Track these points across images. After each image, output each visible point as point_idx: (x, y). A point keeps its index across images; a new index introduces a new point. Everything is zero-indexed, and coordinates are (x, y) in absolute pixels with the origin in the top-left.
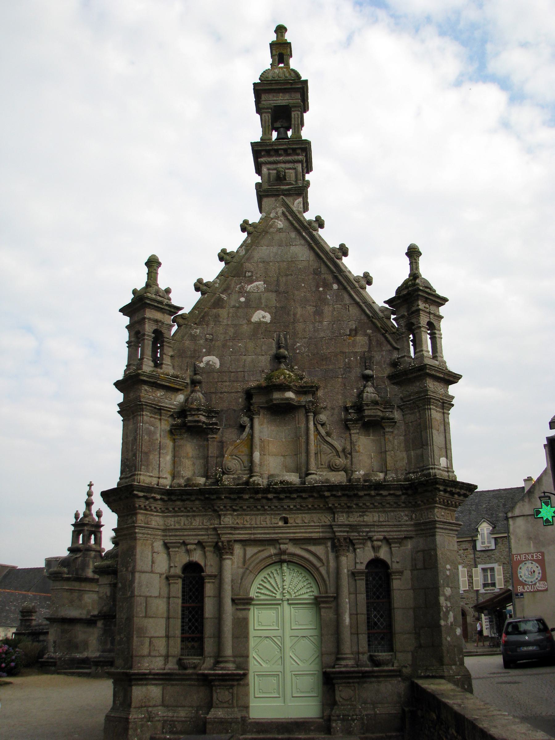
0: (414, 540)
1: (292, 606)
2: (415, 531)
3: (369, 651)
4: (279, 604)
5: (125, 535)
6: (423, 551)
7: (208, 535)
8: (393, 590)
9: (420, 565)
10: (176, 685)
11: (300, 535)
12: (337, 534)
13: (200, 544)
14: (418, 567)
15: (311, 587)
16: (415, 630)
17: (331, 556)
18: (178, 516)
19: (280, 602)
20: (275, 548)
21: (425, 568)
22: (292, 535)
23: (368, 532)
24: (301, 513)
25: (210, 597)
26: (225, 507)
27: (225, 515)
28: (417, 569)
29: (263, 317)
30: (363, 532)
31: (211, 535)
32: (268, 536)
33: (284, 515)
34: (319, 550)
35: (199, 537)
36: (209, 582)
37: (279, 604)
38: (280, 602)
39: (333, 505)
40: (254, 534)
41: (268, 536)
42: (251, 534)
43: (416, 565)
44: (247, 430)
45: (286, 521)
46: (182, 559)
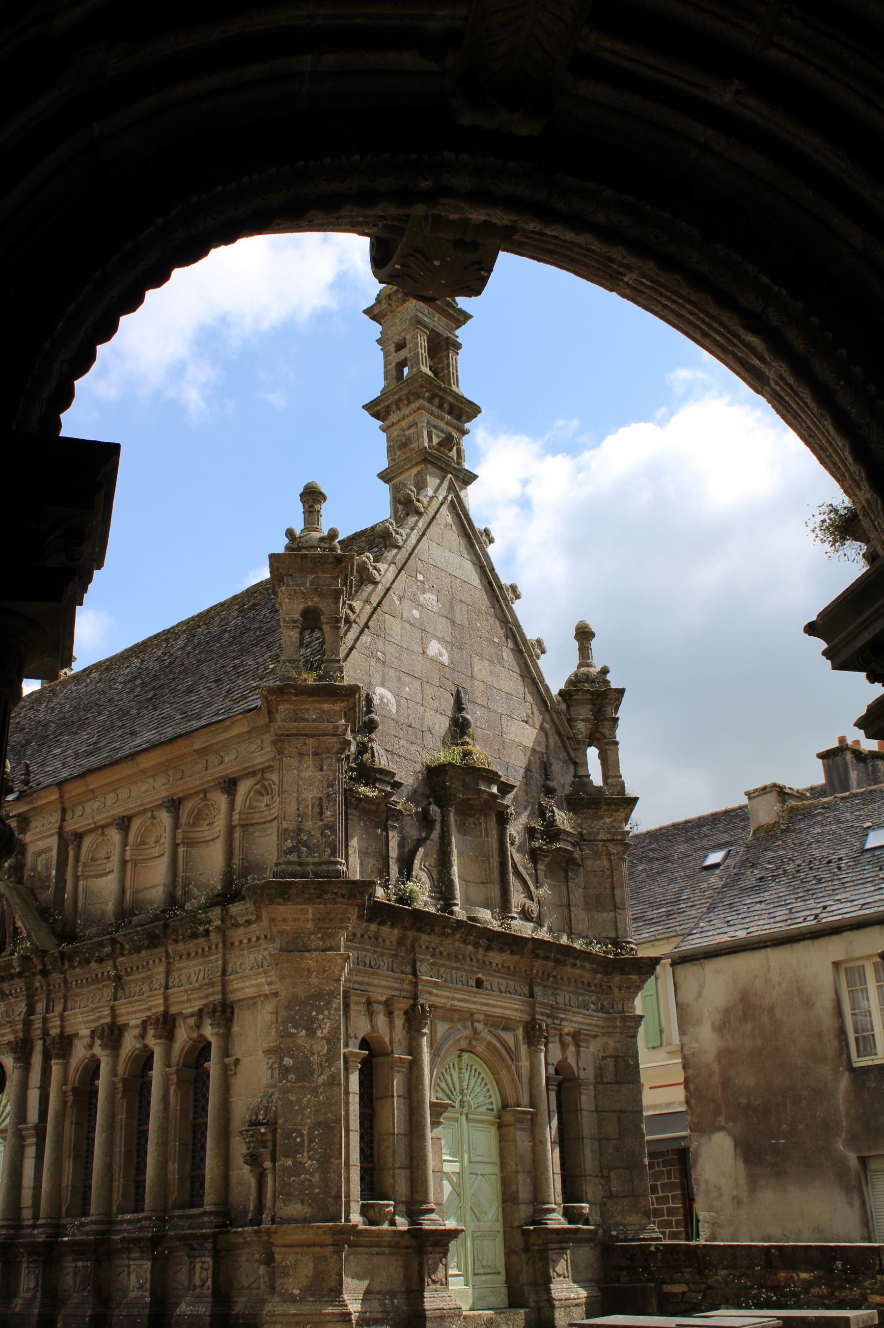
0: (598, 1039)
2: (603, 1027)
3: (564, 1202)
6: (616, 1057)
7: (401, 991)
8: (581, 1110)
9: (609, 1077)
10: (361, 1253)
11: (498, 1010)
12: (538, 1017)
14: (605, 1080)
16: (601, 1171)
17: (523, 1048)
18: (364, 949)
19: (458, 1115)
20: (465, 1027)
21: (618, 1082)
22: (490, 1009)
23: (562, 1020)
24: (497, 977)
28: (604, 1083)
29: (441, 655)
30: (558, 1018)
31: (406, 991)
32: (466, 1005)
33: (480, 975)
34: (508, 1037)
36: (398, 1072)
38: (458, 1115)
39: (537, 972)
40: (453, 999)
41: (466, 1005)
42: (448, 998)
43: (601, 1075)
44: (438, 826)
45: (479, 984)
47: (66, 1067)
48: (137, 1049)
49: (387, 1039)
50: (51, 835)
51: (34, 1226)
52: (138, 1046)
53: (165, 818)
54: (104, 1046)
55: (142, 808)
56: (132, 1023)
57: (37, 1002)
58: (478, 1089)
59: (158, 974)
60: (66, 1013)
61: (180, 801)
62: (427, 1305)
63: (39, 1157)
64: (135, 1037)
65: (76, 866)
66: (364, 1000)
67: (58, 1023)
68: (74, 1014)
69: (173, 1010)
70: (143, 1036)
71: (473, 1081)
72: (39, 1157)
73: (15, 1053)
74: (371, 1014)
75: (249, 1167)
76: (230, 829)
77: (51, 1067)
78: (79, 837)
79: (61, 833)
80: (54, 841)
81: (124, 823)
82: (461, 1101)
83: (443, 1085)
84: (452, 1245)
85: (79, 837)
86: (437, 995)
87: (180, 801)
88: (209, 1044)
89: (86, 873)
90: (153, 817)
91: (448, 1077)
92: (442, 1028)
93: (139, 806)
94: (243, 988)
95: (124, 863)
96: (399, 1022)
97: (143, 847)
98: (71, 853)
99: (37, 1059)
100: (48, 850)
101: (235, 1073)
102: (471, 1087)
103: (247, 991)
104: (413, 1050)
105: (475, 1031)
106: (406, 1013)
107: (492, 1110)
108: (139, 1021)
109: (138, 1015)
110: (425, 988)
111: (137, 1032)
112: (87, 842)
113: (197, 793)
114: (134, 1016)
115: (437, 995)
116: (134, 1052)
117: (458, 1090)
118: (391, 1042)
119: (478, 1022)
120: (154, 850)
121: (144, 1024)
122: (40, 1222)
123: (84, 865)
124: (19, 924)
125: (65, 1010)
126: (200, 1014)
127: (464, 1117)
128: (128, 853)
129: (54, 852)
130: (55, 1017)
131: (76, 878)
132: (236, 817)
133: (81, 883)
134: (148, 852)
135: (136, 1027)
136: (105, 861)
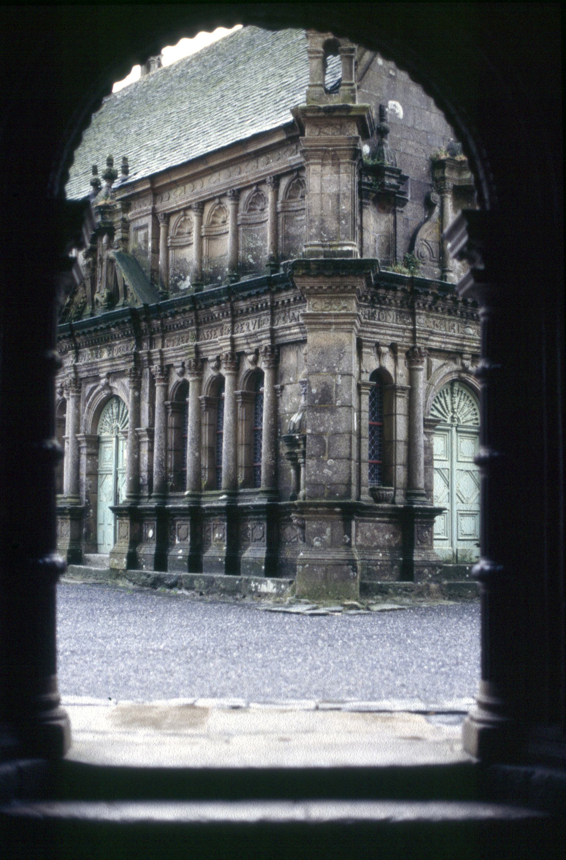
1: (459, 434)
4: (447, 431)
5: (330, 324)
13: (393, 348)
15: (476, 414)
19: (449, 428)
20: (456, 363)
25: (400, 414)
26: (424, 305)
27: (420, 314)
31: (406, 337)
35: (396, 339)
36: (400, 397)
37: (447, 431)
38: (449, 428)
44: (437, 209)
46: (371, 363)
47: (166, 387)
48: (214, 377)
49: (392, 373)
50: (147, 215)
51: (150, 497)
52: (215, 374)
53: (228, 204)
54: (192, 374)
55: (212, 196)
56: (210, 358)
57: (144, 340)
58: (466, 409)
59: (228, 322)
60: (164, 349)
61: (240, 191)
62: (415, 558)
63: (151, 451)
64: (213, 368)
65: (166, 240)
66: (374, 345)
67: (159, 356)
68: (169, 350)
69: (239, 349)
70: (218, 368)
71: (462, 404)
72: (151, 451)
73: (130, 377)
74: (380, 355)
75: (290, 462)
76: (276, 214)
77: (155, 388)
78: (168, 216)
79: (154, 213)
80: (148, 220)
81: (201, 206)
82: (452, 417)
83: (438, 406)
84: (438, 518)
85: (168, 216)
86: (433, 341)
87: (240, 191)
88: (262, 374)
89: (175, 245)
90: (220, 203)
91: (442, 400)
92: (436, 362)
93: (209, 195)
94: (285, 335)
95: (200, 238)
96: (402, 362)
97: (214, 225)
98: (162, 230)
99: (146, 384)
100: (146, 226)
101: (281, 396)
102: (461, 407)
103: (288, 337)
104: (412, 379)
105: (463, 365)
106: (407, 353)
107: (477, 424)
108: (215, 357)
109: (214, 352)
110: (422, 336)
111: (213, 364)
112: (173, 220)
113: (250, 187)
114: (211, 353)
115: (433, 341)
116: (212, 378)
117: (450, 409)
118: (396, 374)
119: (467, 359)
120: (222, 228)
121: (218, 359)
122: (153, 494)
123: (172, 238)
124: (127, 283)
125: (163, 347)
126: (257, 353)
127: (454, 429)
128: (203, 230)
129: (150, 230)
130: (155, 352)
131: (167, 249)
132: (279, 205)
133: (170, 252)
134: (217, 229)
135: (212, 361)
136: (187, 235)
